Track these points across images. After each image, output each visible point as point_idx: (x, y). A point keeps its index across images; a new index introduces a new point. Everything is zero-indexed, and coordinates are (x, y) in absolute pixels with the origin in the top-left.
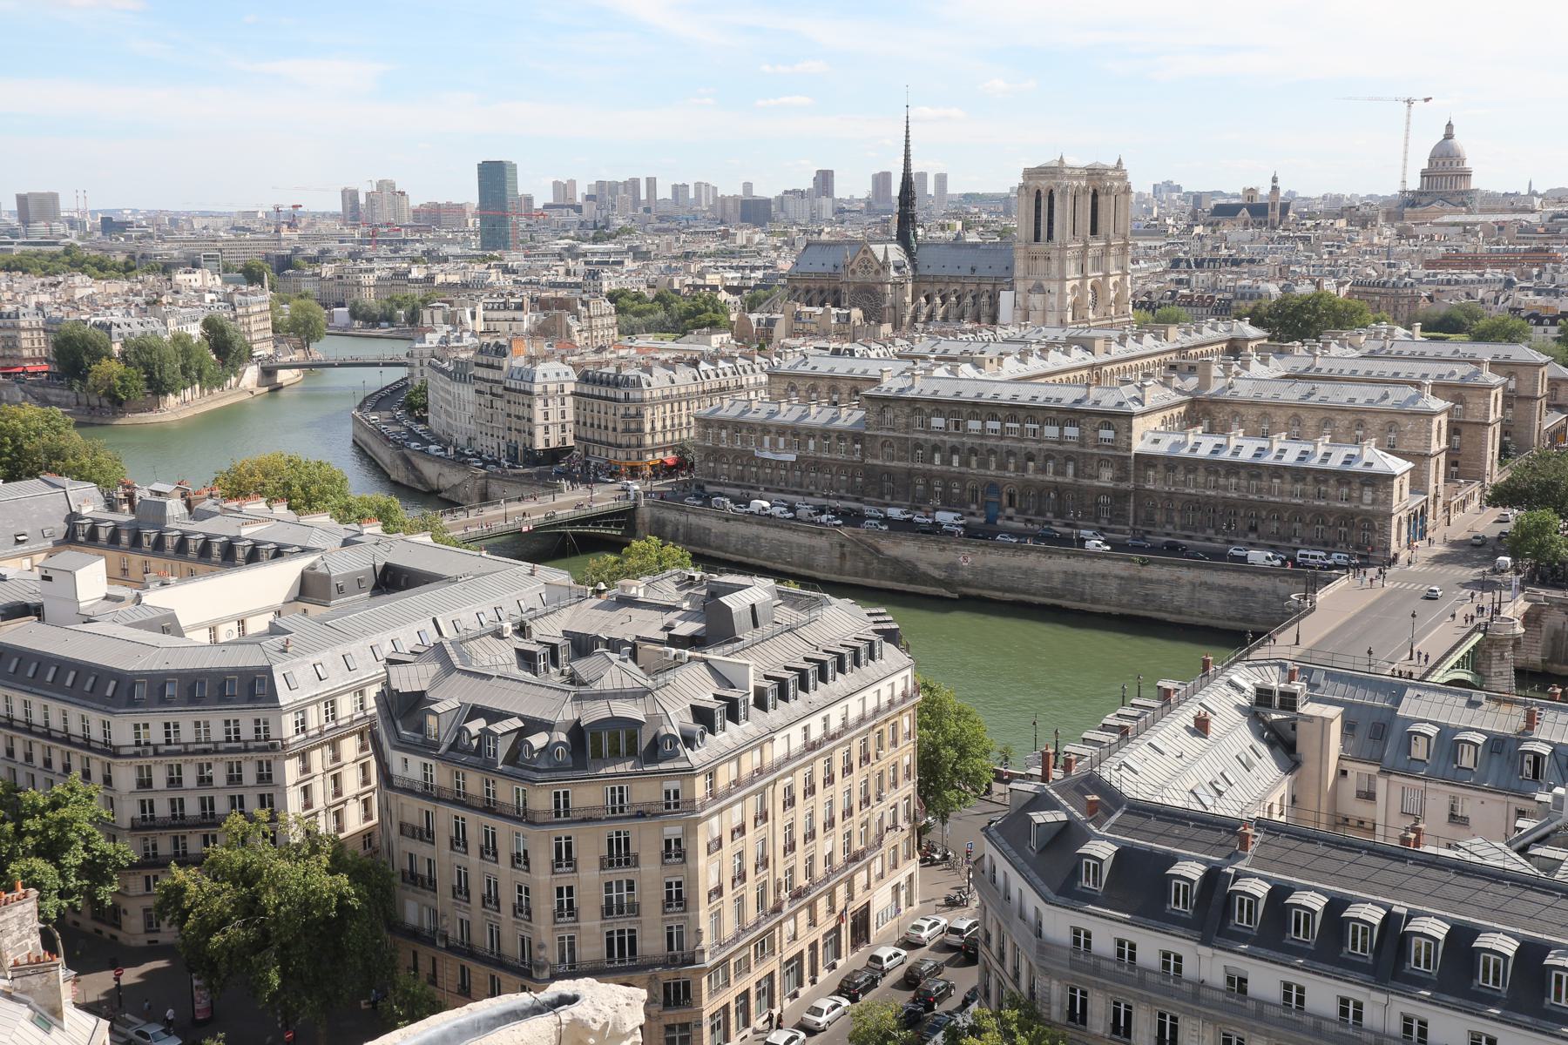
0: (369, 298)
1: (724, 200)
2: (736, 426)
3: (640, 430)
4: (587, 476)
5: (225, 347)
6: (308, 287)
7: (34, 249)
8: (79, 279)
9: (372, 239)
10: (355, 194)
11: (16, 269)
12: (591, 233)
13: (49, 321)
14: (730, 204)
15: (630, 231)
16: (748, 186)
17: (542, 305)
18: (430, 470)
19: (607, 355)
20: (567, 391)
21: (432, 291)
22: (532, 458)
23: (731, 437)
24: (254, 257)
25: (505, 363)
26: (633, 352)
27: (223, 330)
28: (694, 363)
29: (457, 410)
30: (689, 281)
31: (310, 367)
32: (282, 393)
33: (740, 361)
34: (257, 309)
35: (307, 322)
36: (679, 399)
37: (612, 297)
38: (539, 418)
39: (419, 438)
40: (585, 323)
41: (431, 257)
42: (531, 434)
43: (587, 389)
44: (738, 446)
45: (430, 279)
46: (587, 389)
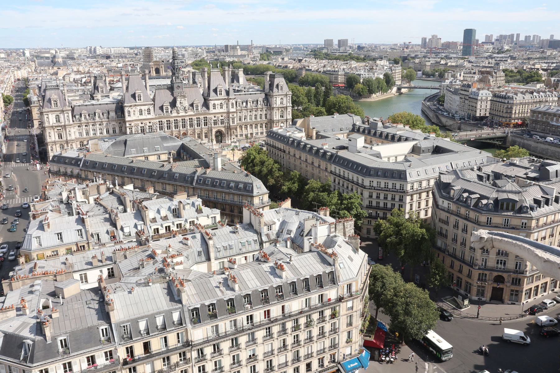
0: (428, 69)
1: (543, 41)
2: (544, 113)
3: (511, 113)
4: (491, 126)
5: (388, 81)
6: (411, 65)
7: (341, 54)
8: (353, 62)
9: (431, 52)
10: (425, 39)
11: (337, 59)
12: (497, 51)
13: (346, 73)
14: (545, 42)
15: (510, 51)
16: (552, 36)
17: (482, 73)
18: (444, 120)
19: (501, 89)
20: (489, 99)
21: (447, 68)
22: (475, 118)
23: (542, 117)
24: (397, 57)
25: (470, 90)
26: (510, 88)
27: (389, 77)
28: (532, 93)
29: (453, 103)
30: (529, 67)
31: (410, 88)
32: (402, 95)
33: (548, 93)
34: (398, 71)
35: (411, 75)
36: (525, 104)
37: (504, 71)
38: (479, 107)
39: (441, 110)
40: (495, 79)
41: (447, 57)
42: (476, 111)
43: (495, 99)
44: (544, 120)
45: (446, 64)
46: (495, 99)
